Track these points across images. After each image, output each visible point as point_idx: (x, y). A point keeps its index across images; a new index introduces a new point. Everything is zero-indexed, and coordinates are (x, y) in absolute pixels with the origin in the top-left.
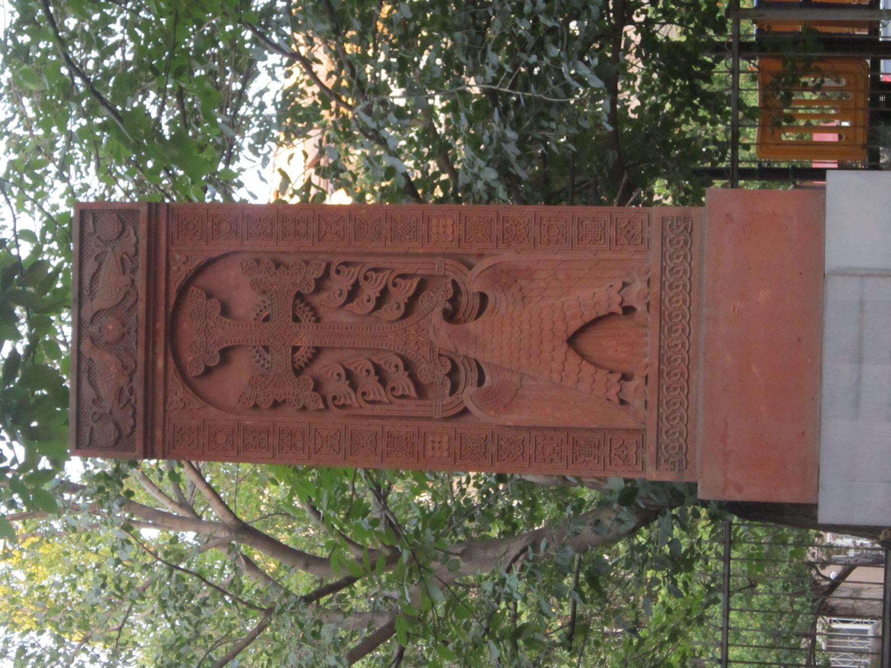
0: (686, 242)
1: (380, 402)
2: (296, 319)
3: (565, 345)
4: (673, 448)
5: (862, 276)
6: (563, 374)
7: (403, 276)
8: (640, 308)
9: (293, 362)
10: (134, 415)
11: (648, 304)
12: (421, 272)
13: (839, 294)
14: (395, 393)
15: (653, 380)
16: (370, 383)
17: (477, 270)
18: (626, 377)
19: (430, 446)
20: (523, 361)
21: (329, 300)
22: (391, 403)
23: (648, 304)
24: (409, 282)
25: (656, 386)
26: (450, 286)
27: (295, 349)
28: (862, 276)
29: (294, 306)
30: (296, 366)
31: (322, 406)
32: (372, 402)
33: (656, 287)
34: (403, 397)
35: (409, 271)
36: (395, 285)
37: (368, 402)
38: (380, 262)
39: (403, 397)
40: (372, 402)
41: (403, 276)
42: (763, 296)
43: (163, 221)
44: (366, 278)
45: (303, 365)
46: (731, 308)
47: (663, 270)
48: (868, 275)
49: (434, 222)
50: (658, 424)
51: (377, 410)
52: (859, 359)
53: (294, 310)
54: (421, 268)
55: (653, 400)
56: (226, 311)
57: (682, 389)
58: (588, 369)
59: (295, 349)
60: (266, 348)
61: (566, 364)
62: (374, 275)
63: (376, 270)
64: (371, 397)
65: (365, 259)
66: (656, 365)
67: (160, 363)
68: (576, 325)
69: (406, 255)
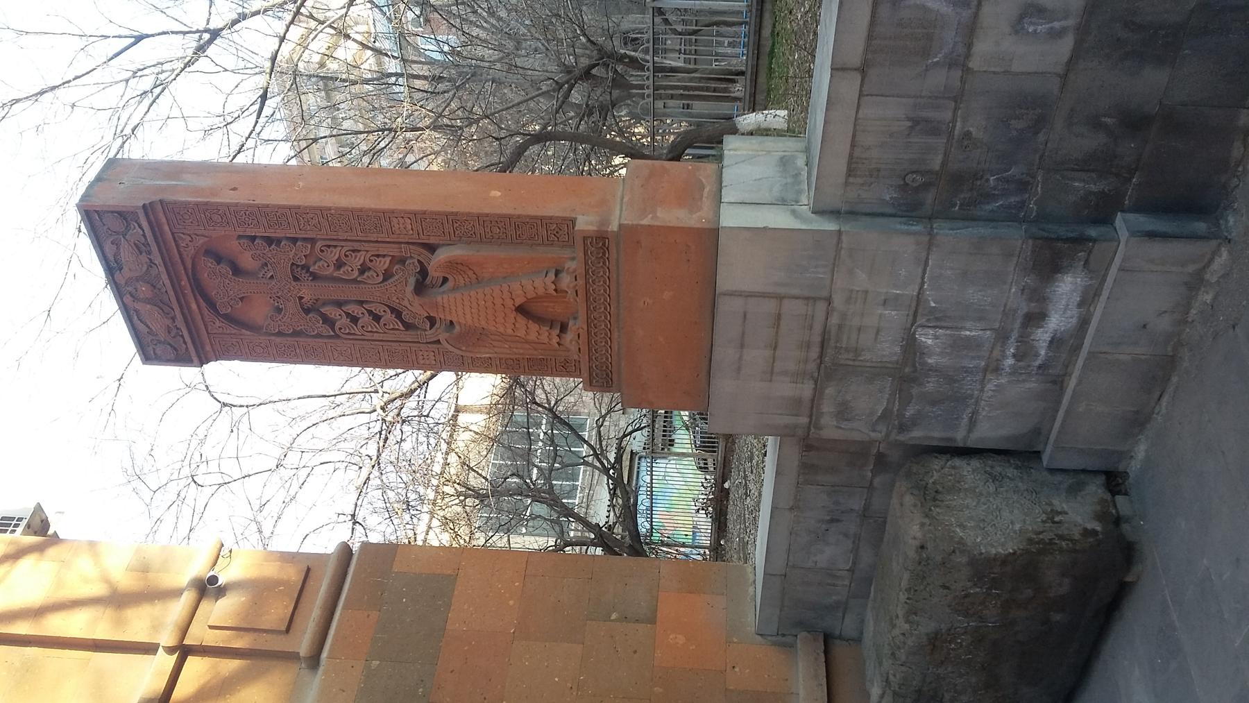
7: (378, 256)
10: (185, 343)
18: (564, 328)
27: (301, 298)
29: (292, 271)
33: (581, 282)
38: (356, 246)
41: (378, 256)
43: (161, 216)
51: (376, 336)
55: (585, 348)
56: (237, 271)
58: (534, 327)
59: (301, 298)
63: (354, 251)
67: (194, 306)
69: (377, 242)
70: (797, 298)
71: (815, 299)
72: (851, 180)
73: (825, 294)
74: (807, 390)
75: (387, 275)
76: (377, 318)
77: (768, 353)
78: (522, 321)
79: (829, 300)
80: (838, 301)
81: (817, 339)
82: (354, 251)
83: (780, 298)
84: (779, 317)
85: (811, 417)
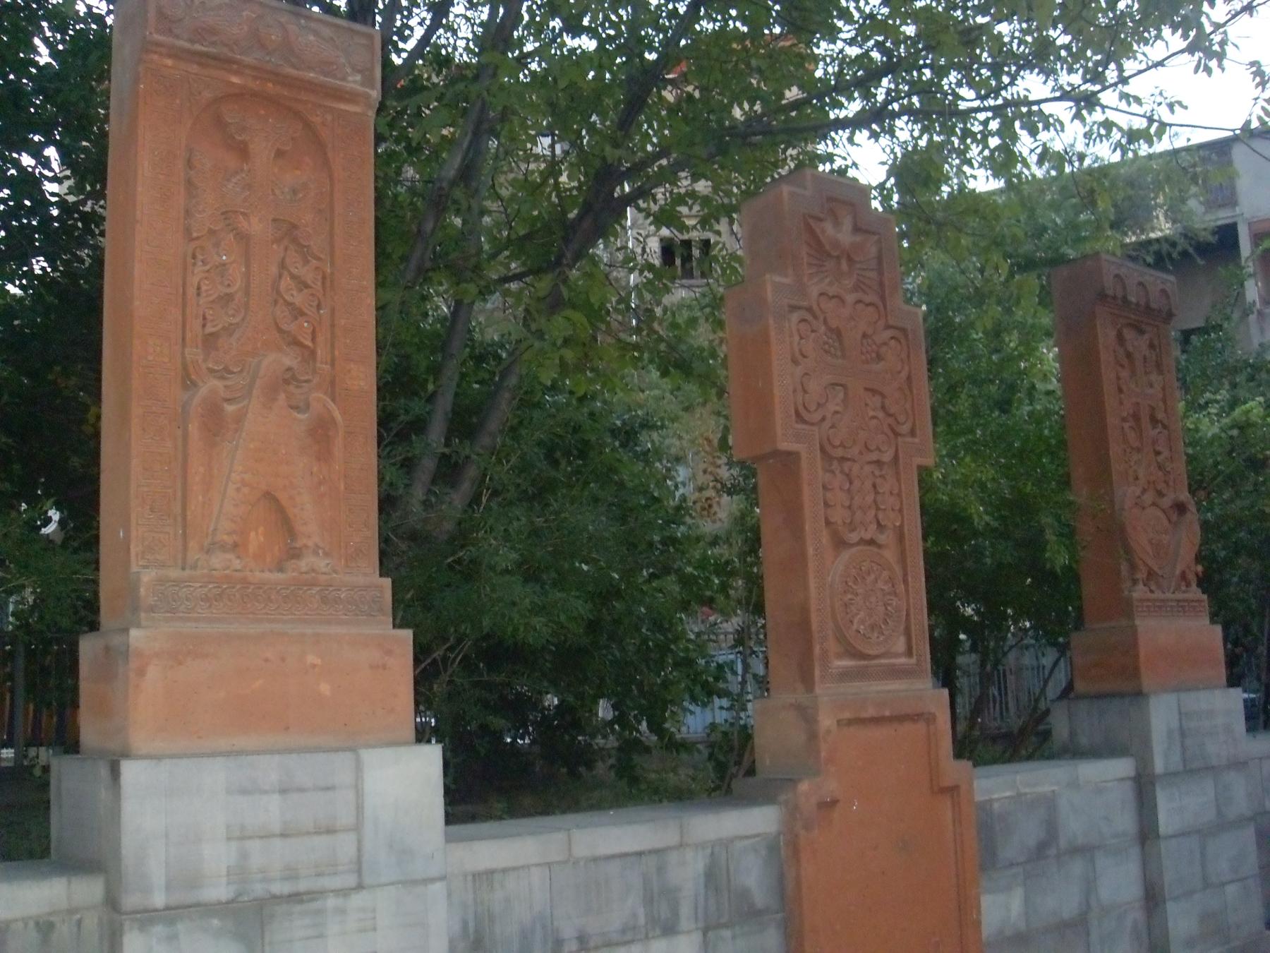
5: (356, 786)
8: (303, 564)
13: (340, 765)
17: (332, 405)
28: (356, 786)
42: (325, 688)
48: (357, 792)
52: (283, 791)
70: (359, 850)
71: (359, 872)
72: (470, 878)
73: (368, 880)
74: (218, 892)
77: (277, 828)
79: (360, 887)
80: (357, 900)
81: (302, 886)
83: (357, 828)
84: (330, 831)
85: (168, 908)
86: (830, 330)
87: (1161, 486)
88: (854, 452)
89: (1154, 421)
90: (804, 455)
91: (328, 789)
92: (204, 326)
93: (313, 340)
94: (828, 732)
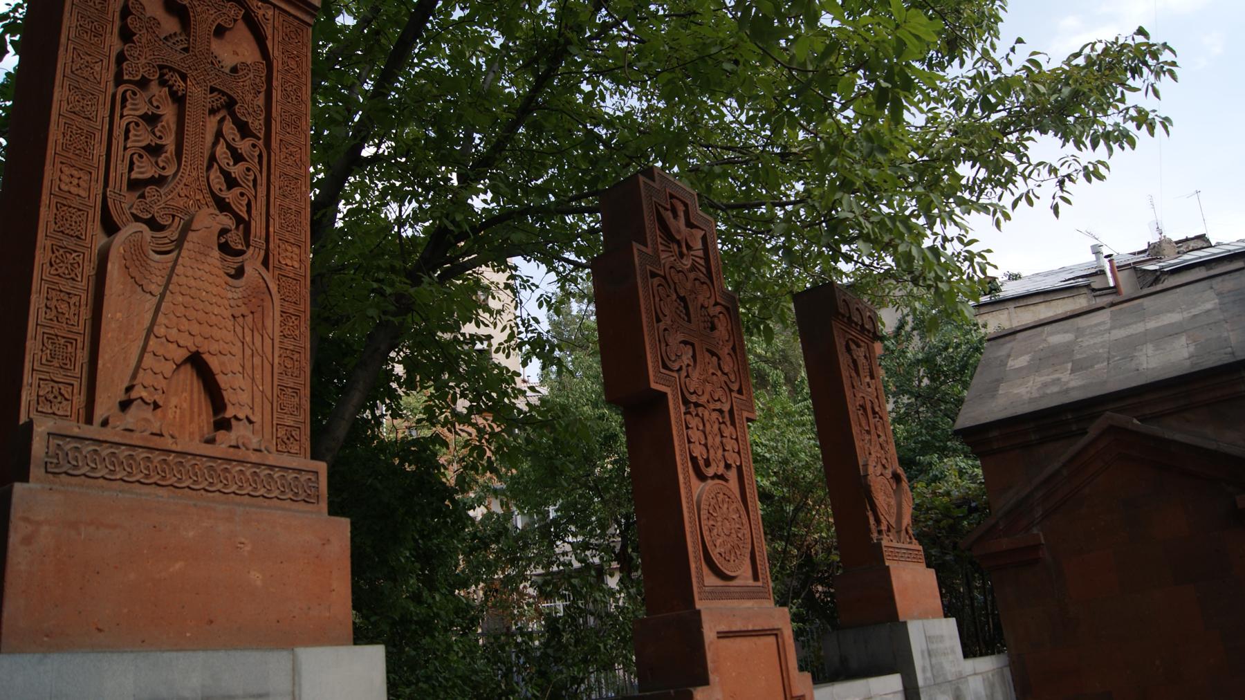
0: (296, 494)
1: (127, 138)
2: (213, 90)
3: (194, 349)
4: (76, 459)
5: (293, 693)
6: (164, 340)
7: (249, 205)
8: (232, 437)
9: (171, 69)
11: (237, 447)
12: (253, 223)
14: (136, 156)
15: (157, 442)
16: (143, 137)
19: (75, 173)
20: (180, 299)
21: (229, 129)
22: (125, 148)
23: (237, 447)
24: (245, 209)
25: (151, 445)
26: (240, 247)
29: (224, 94)
30: (165, 71)
31: (126, 77)
32: (127, 131)
33: (254, 458)
34: (132, 163)
35: (254, 212)
36: (242, 194)
37: (128, 124)
39: (132, 163)
40: (127, 131)
41: (249, 205)
42: (256, 577)
43: (299, 14)
44: (249, 170)
45: (167, 77)
46: (243, 540)
47: (271, 467)
49: (296, 250)
50: (106, 442)
53: (220, 92)
54: (257, 226)
55: (135, 439)
57: (147, 476)
59: (184, 77)
60: (186, 50)
61: (175, 346)
62: (251, 178)
64: (132, 132)
65: (264, 174)
66: (174, 448)
68: (214, 363)
75: (223, 206)
76: (154, 150)
78: (181, 355)
82: (255, 181)
86: (678, 296)
87: (884, 461)
88: (703, 400)
89: (874, 413)
90: (670, 397)
91: (260, 696)
92: (131, 169)
93: (249, 212)
94: (711, 643)
